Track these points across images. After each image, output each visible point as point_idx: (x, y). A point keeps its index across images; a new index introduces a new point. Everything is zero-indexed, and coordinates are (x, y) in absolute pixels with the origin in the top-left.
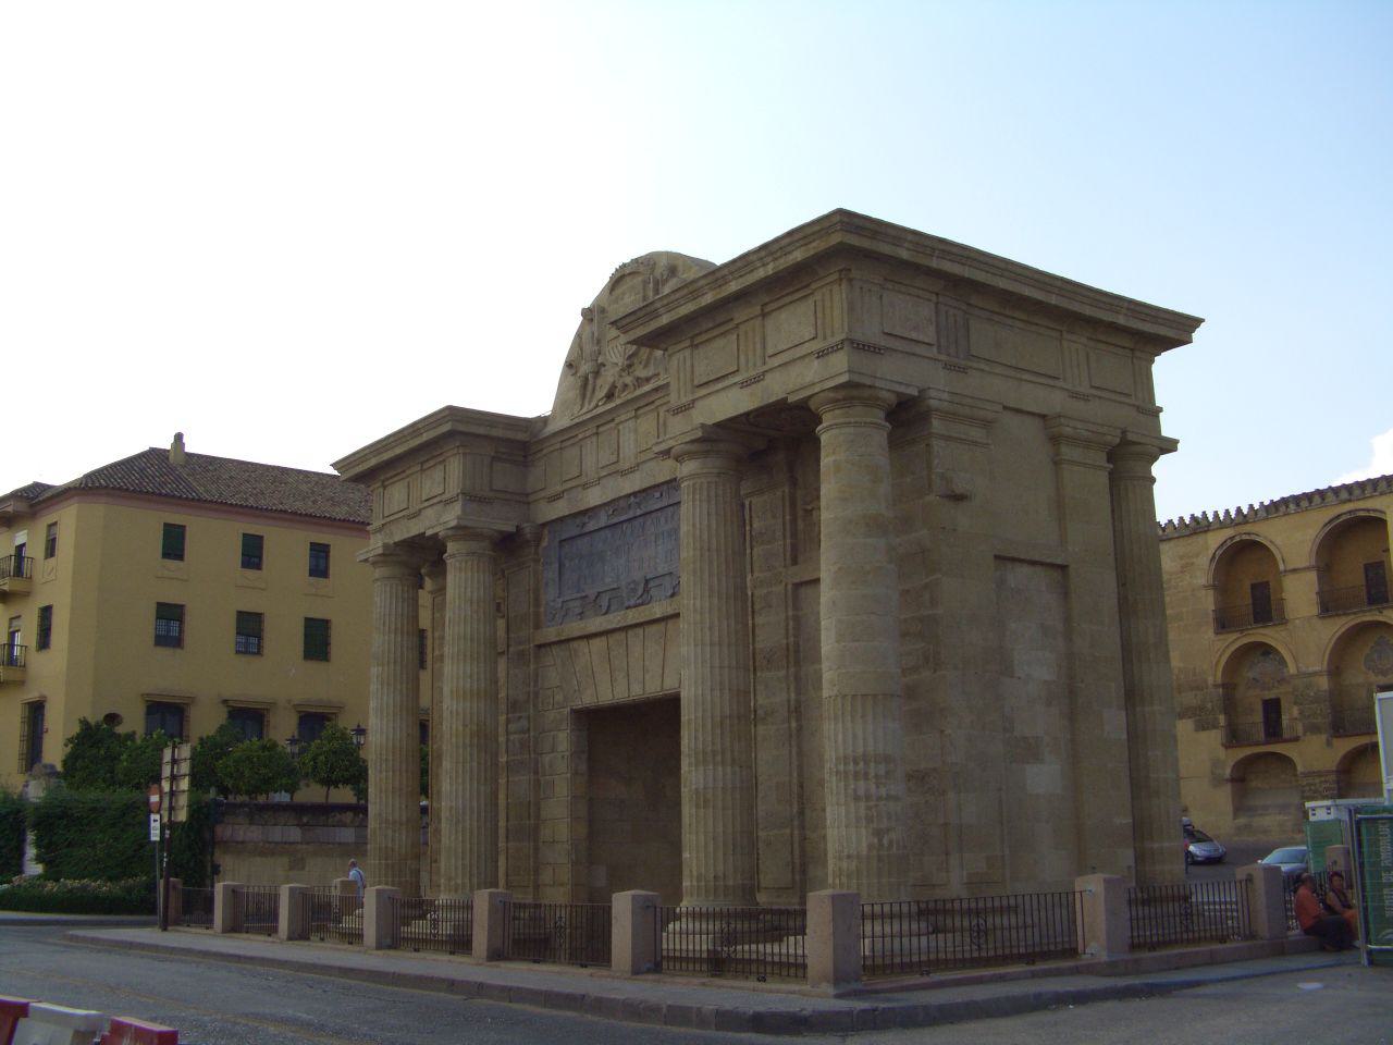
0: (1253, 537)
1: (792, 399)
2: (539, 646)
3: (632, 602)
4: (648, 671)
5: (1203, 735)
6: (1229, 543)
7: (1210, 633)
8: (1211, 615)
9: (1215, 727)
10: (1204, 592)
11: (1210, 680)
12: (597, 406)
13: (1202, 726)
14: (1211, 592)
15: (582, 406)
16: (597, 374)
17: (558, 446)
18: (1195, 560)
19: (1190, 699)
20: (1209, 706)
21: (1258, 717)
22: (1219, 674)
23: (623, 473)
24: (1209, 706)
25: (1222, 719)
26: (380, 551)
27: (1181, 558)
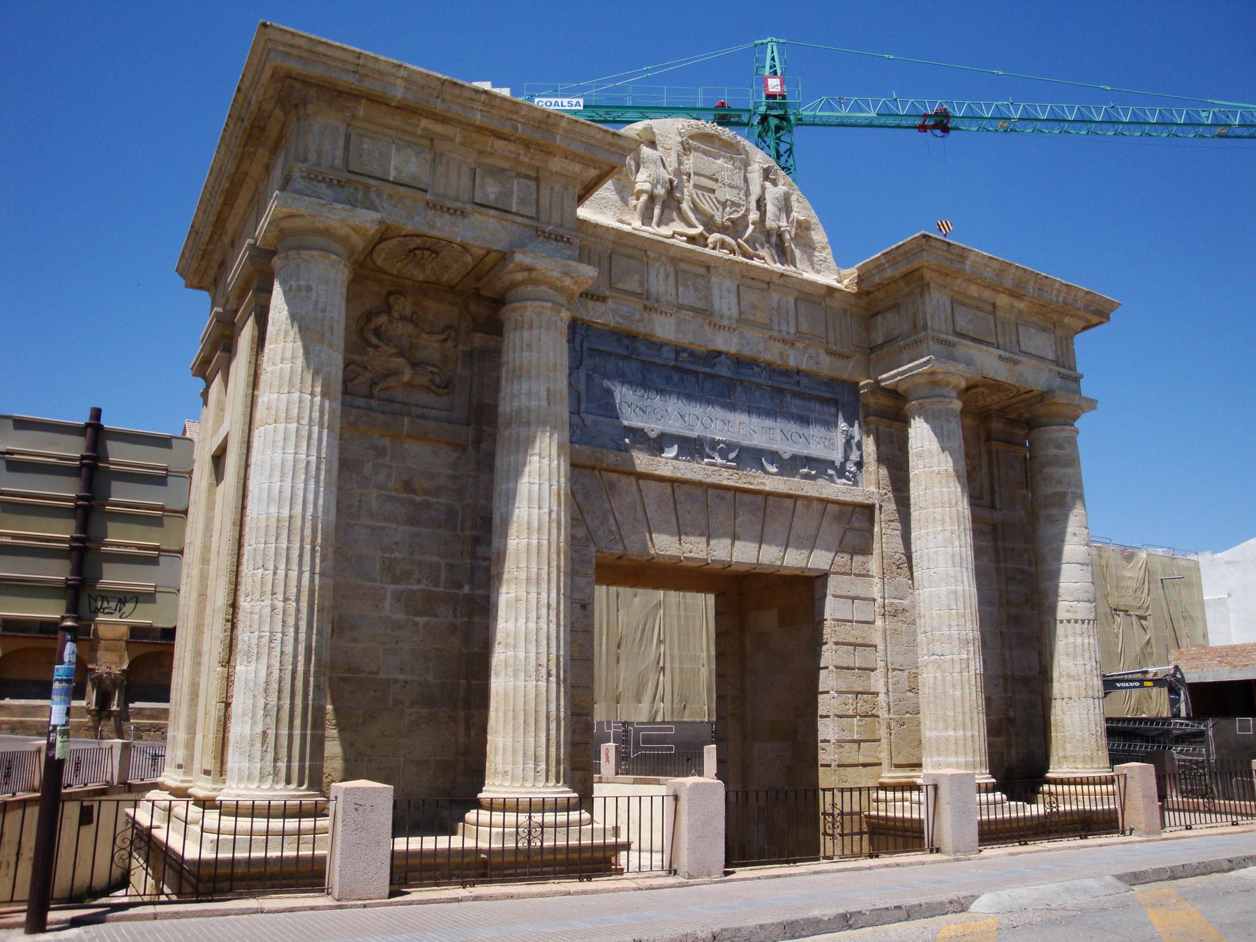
12: (673, 237)
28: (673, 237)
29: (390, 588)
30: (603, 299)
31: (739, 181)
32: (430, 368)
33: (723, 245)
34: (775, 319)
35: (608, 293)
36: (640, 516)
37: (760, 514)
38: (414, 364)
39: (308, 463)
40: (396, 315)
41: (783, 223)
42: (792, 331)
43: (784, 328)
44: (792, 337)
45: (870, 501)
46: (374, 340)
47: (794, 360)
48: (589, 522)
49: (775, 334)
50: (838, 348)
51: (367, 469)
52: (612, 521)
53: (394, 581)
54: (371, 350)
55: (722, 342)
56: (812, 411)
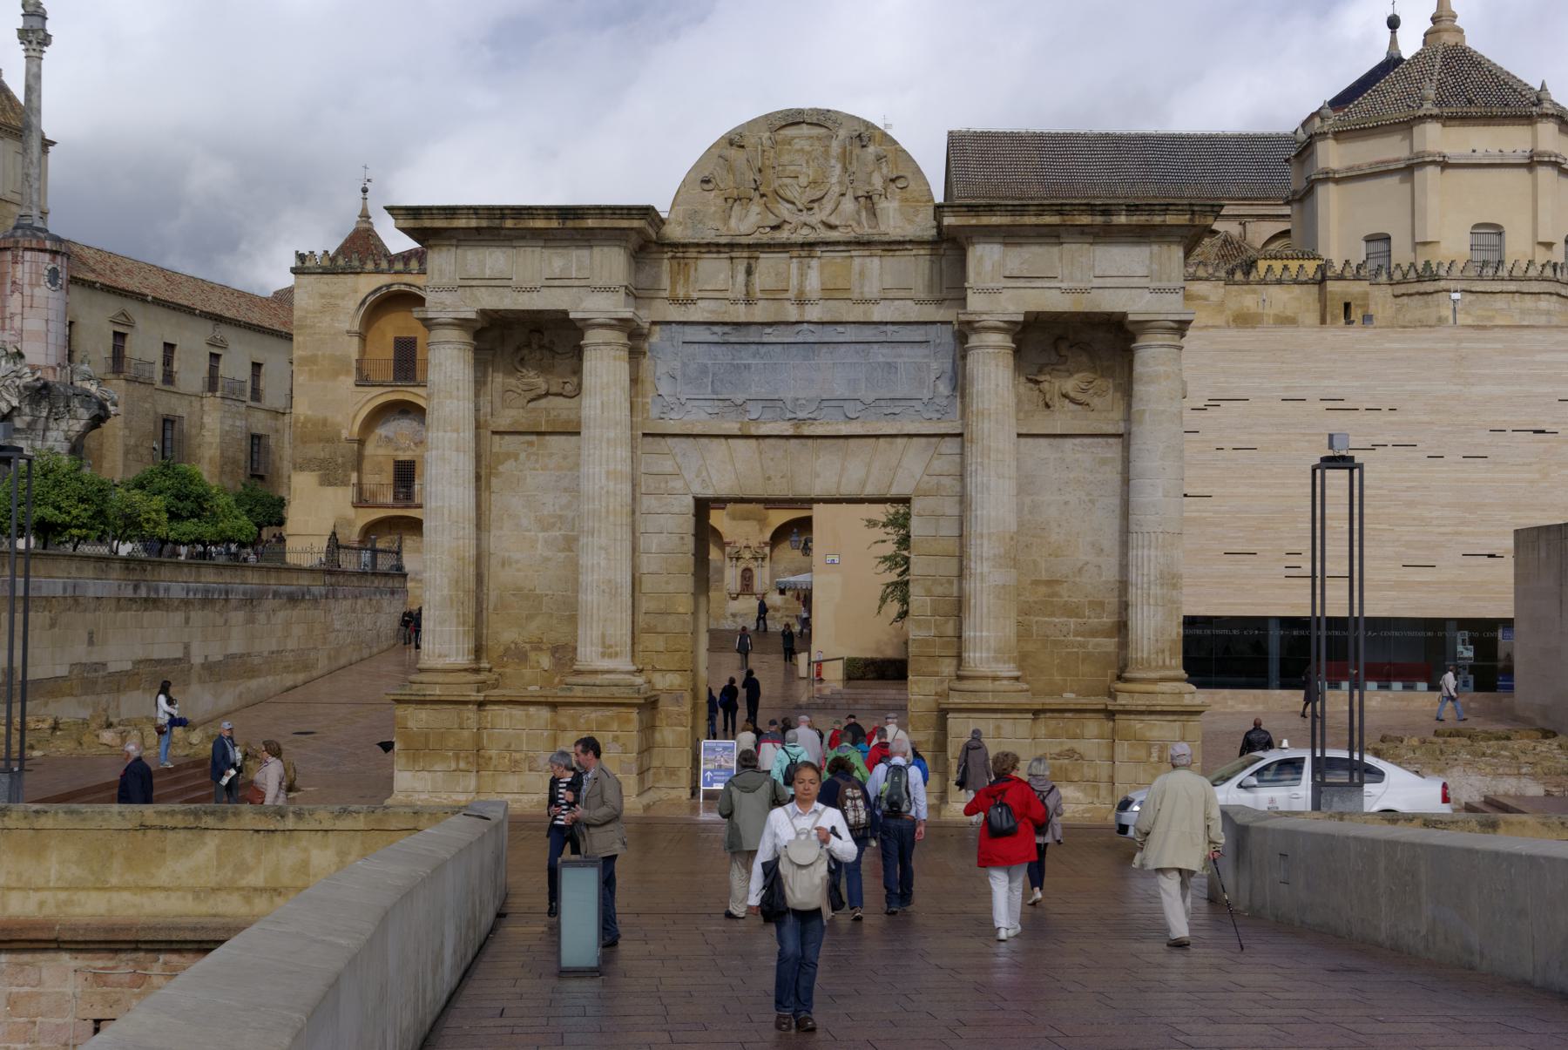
0: (414, 290)
1: (1131, 317)
3: (801, 415)
4: (817, 476)
5: (330, 491)
6: (384, 291)
9: (345, 483)
10: (347, 338)
11: (345, 434)
13: (328, 480)
14: (356, 340)
19: (318, 451)
20: (340, 460)
21: (388, 477)
22: (356, 428)
24: (340, 460)
26: (473, 316)
27: (323, 296)
29: (541, 535)
30: (693, 302)
40: (535, 346)
43: (866, 289)
44: (876, 295)
47: (877, 313)
49: (856, 296)
51: (523, 456)
53: (544, 529)
56: (900, 356)
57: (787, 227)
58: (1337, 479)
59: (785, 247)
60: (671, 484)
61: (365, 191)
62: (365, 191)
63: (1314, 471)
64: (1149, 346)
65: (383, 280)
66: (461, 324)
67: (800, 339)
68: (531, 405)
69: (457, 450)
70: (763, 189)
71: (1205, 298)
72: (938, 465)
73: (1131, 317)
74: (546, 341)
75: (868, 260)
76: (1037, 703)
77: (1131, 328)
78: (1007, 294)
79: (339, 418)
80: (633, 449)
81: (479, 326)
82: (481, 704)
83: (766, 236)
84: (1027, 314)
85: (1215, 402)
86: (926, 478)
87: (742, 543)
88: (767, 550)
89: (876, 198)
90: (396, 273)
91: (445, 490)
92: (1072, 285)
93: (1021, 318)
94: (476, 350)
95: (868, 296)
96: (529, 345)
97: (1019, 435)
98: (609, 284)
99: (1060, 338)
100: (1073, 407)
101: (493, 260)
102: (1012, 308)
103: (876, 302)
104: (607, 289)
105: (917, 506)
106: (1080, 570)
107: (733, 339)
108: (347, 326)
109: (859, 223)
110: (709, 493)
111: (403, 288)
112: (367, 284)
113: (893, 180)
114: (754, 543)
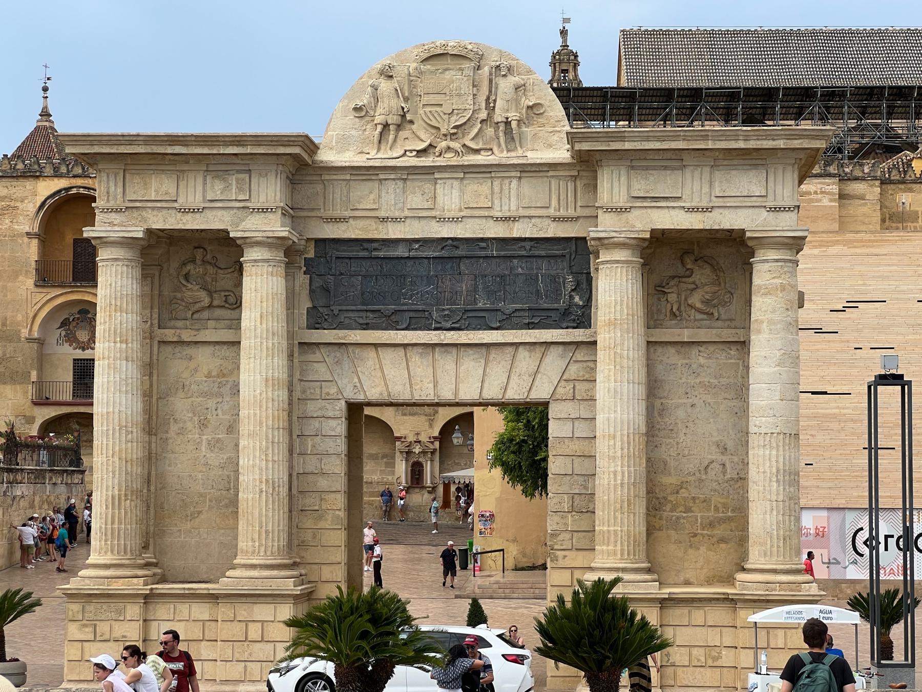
1: (748, 234)
2: (299, 343)
3: (444, 324)
6: (63, 194)
7: (30, 282)
8: (33, 264)
10: (26, 239)
11: (25, 333)
12: (404, 155)
14: (35, 242)
15: (379, 150)
16: (399, 127)
17: (348, 177)
18: (18, 204)
21: (67, 376)
23: (441, 220)
25: (34, 375)
26: (140, 235)
28: (404, 155)
30: (345, 220)
31: (466, 88)
32: (223, 294)
33: (449, 148)
34: (497, 202)
35: (347, 214)
36: (380, 374)
37: (483, 361)
38: (210, 294)
39: (115, 382)
40: (199, 262)
41: (513, 115)
42: (513, 208)
43: (505, 208)
45: (592, 339)
46: (184, 283)
48: (339, 382)
50: (563, 213)
52: (356, 380)
54: (184, 289)
55: (446, 231)
57: (431, 151)
58: (889, 395)
59: (429, 171)
60: (325, 390)
61: (45, 89)
62: (45, 89)
63: (869, 387)
64: (767, 261)
65: (62, 183)
66: (128, 243)
67: (444, 253)
68: (195, 316)
69: (127, 360)
70: (408, 117)
71: (862, 198)
72: (574, 370)
73: (748, 234)
74: (209, 257)
75: (507, 181)
76: (666, 591)
77: (750, 243)
78: (635, 213)
79: (19, 317)
80: (291, 356)
81: (145, 243)
82: (146, 597)
83: (411, 161)
84: (653, 231)
85: (853, 304)
86: (563, 383)
87: (411, 438)
88: (437, 444)
89: (514, 124)
90: (74, 176)
91: (113, 399)
92: (694, 204)
93: (648, 236)
94: (144, 267)
95: (508, 214)
96: (193, 261)
97: (648, 342)
98: (266, 205)
99: (686, 252)
100: (699, 316)
101: (159, 186)
102: (639, 226)
103: (515, 219)
104: (264, 210)
105: (554, 411)
106: (706, 468)
107: (381, 254)
108: (27, 229)
109: (499, 145)
110: (360, 398)
111: (82, 191)
112: (47, 187)
113: (530, 108)
114: (424, 438)
